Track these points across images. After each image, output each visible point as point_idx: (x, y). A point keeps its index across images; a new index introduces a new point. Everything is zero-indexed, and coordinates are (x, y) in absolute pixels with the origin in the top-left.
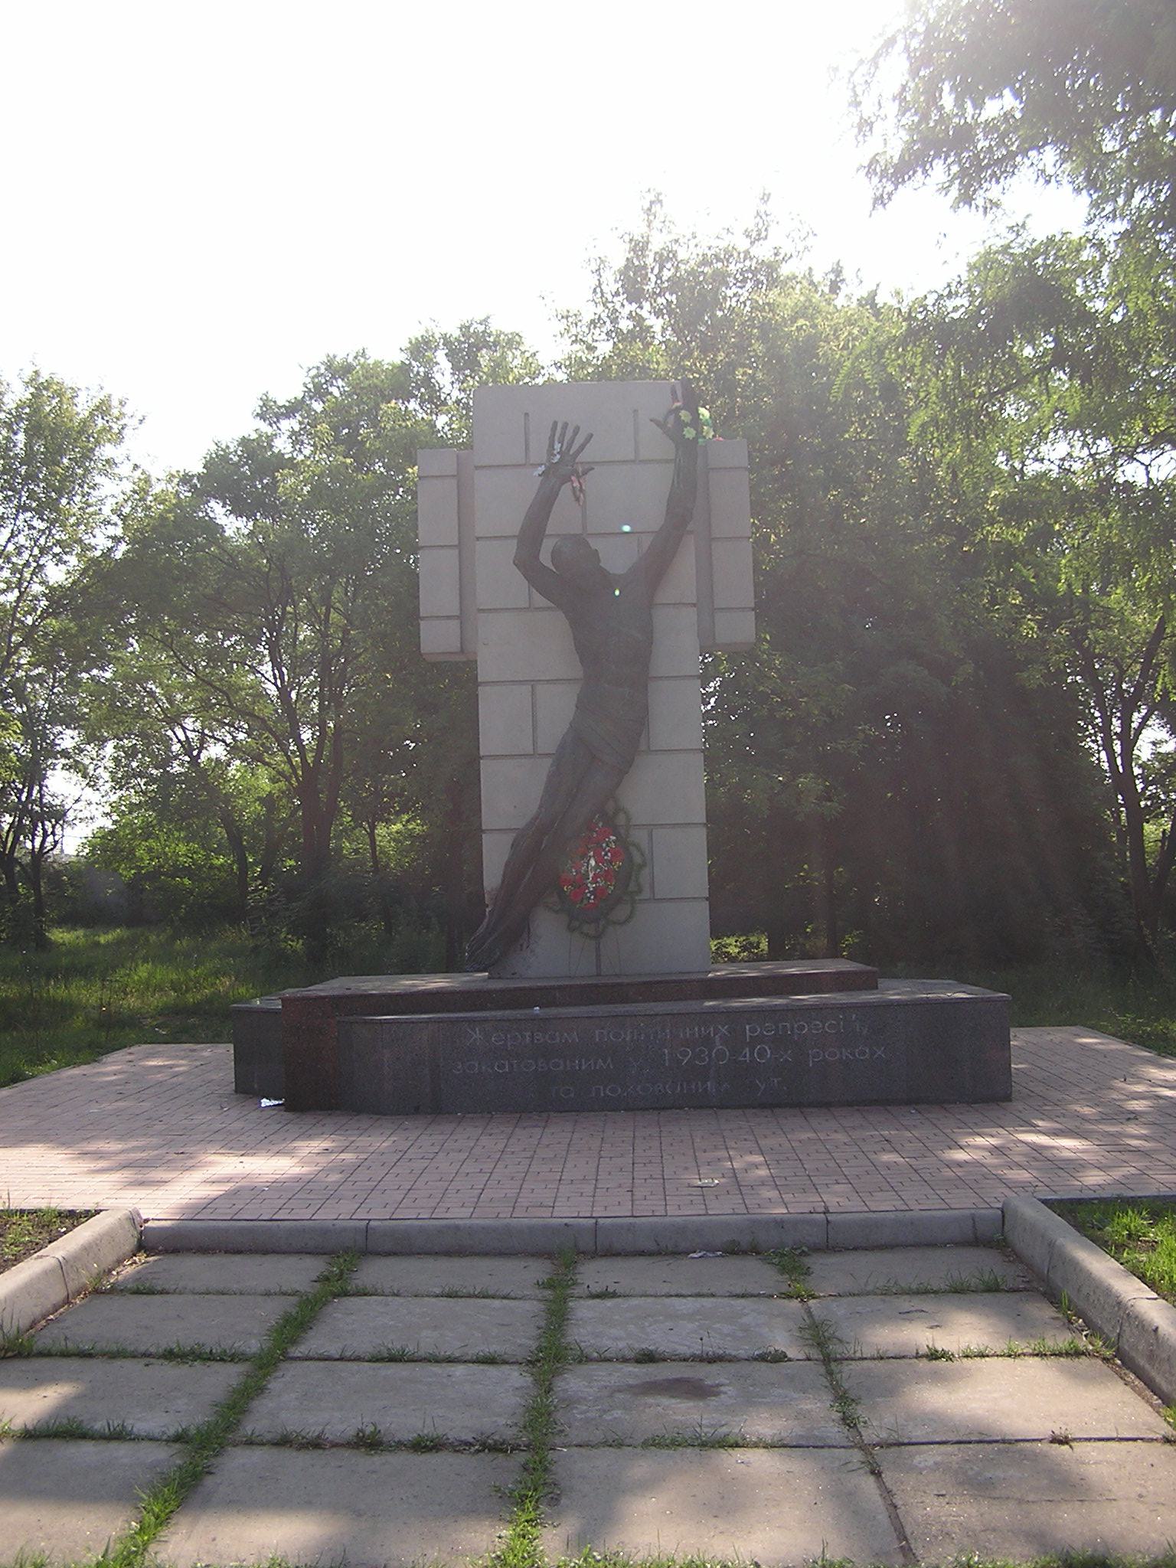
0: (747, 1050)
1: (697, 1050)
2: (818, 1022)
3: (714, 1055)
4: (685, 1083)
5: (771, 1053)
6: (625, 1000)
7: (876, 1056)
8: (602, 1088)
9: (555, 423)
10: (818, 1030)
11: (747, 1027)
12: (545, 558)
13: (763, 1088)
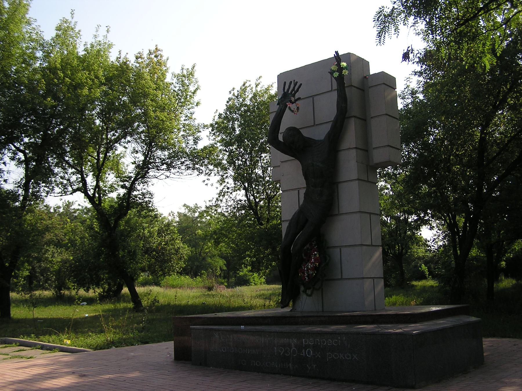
0: (304, 351)
1: (286, 349)
2: (330, 340)
3: (292, 351)
4: (282, 364)
5: (313, 353)
6: (296, 324)
7: (354, 358)
8: (254, 362)
9: (285, 83)
10: (330, 344)
11: (304, 340)
12: (281, 138)
13: (309, 369)
